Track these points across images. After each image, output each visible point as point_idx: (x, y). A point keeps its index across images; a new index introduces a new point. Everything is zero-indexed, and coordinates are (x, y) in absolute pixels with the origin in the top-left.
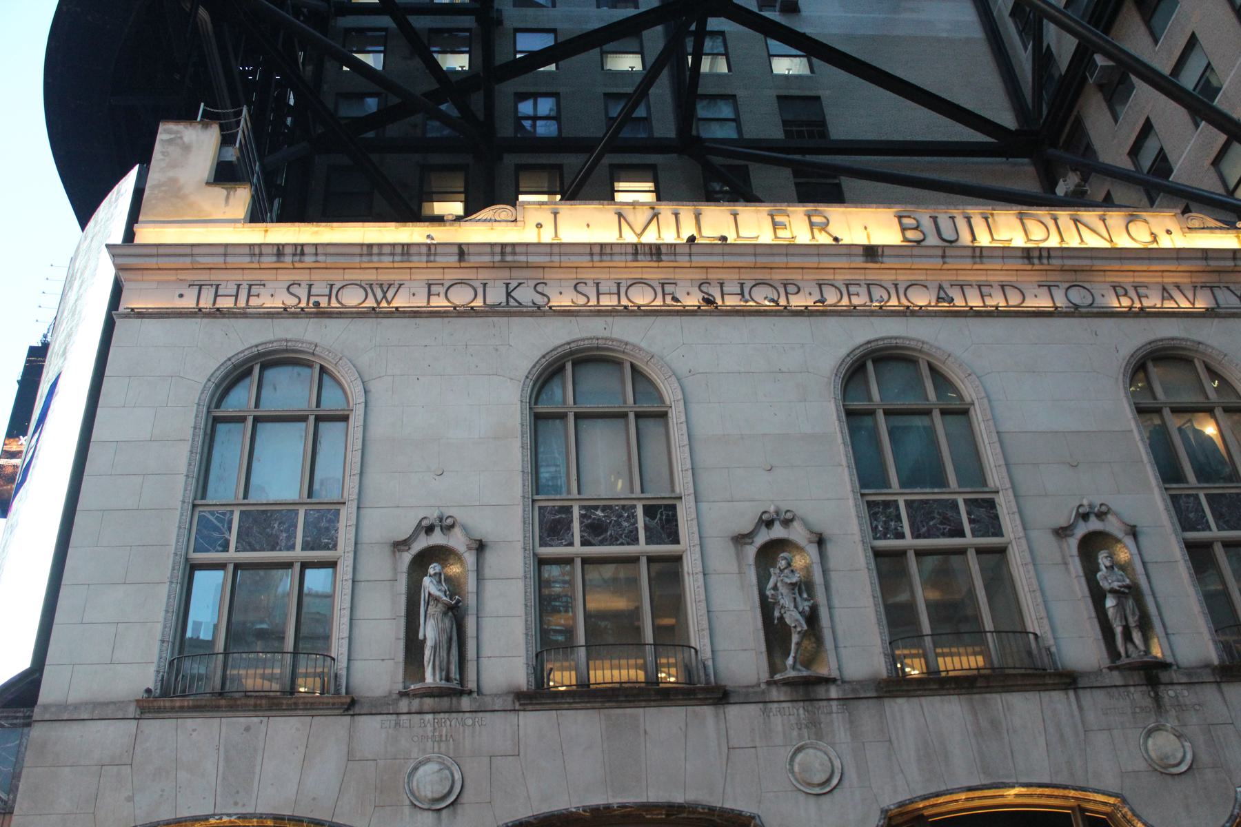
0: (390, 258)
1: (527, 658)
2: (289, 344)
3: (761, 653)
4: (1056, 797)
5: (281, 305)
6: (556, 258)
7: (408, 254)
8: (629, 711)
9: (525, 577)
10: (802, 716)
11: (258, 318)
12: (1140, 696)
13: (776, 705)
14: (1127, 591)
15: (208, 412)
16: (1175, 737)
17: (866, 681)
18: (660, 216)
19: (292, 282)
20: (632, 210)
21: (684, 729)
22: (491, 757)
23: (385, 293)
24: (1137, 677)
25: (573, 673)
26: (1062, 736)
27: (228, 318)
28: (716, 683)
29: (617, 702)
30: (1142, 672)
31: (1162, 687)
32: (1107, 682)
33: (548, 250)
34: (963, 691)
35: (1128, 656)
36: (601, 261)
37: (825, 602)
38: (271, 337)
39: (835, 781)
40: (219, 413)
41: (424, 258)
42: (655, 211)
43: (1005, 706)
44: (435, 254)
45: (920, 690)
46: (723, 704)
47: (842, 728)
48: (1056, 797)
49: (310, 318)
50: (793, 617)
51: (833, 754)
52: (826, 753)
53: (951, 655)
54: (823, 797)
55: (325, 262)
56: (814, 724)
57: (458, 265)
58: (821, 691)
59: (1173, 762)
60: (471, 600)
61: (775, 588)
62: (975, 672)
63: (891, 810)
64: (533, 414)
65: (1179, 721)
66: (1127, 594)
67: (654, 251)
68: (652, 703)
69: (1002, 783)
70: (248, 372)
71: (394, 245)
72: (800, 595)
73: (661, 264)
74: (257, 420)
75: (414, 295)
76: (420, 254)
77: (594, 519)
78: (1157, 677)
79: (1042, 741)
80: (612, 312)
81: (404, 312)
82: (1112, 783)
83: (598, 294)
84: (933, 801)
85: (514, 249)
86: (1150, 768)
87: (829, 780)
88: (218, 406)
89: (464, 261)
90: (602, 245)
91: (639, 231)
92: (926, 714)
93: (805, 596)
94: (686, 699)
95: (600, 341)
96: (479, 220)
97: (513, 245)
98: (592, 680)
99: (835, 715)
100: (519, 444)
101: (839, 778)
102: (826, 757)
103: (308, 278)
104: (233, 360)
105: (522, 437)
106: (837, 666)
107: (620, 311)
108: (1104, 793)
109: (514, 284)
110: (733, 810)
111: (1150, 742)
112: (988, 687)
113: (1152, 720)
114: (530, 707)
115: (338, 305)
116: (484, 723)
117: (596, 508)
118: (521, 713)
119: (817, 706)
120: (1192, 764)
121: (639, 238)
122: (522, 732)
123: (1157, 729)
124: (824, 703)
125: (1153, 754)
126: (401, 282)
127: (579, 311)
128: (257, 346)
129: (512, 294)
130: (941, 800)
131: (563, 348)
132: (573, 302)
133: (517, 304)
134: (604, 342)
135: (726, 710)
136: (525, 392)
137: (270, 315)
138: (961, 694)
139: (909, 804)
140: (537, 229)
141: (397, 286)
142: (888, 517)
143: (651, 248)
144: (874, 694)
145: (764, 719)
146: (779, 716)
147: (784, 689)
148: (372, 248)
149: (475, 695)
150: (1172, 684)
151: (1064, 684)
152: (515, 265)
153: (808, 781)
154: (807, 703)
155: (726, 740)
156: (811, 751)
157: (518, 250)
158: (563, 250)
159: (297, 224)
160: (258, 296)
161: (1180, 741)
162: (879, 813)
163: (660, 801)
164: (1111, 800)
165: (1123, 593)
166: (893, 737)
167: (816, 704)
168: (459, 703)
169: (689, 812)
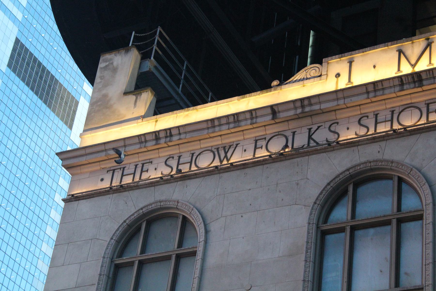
0: (226, 127)
2: (162, 204)
5: (325, 142)
6: (341, 102)
7: (238, 121)
11: (145, 187)
15: (318, 227)
18: (433, 45)
19: (169, 157)
20: (410, 45)
23: (226, 153)
27: (128, 191)
33: (334, 96)
36: (375, 97)
38: (152, 200)
40: (325, 227)
41: (249, 122)
42: (430, 41)
44: (256, 117)
49: (177, 181)
55: (185, 138)
57: (273, 122)
64: (319, 233)
67: (416, 79)
70: (345, 193)
71: (227, 116)
73: (425, 88)
74: (400, 221)
75: (245, 151)
76: (246, 119)
80: (386, 137)
81: (237, 166)
83: (376, 123)
85: (310, 101)
88: (326, 221)
89: (276, 118)
90: (374, 84)
91: (413, 62)
95: (372, 164)
96: (295, 81)
97: (309, 98)
100: (303, 258)
103: (178, 151)
104: (127, 222)
105: (307, 252)
107: (391, 135)
109: (315, 127)
115: (196, 168)
121: (413, 68)
126: (237, 143)
127: (359, 141)
128: (142, 209)
129: (313, 137)
131: (344, 175)
132: (356, 134)
133: (315, 144)
134: (375, 163)
136: (313, 215)
137: (154, 184)
140: (336, 79)
141: (235, 146)
143: (413, 78)
148: (214, 122)
152: (315, 113)
157: (313, 101)
158: (346, 94)
159: (175, 112)
160: (147, 171)
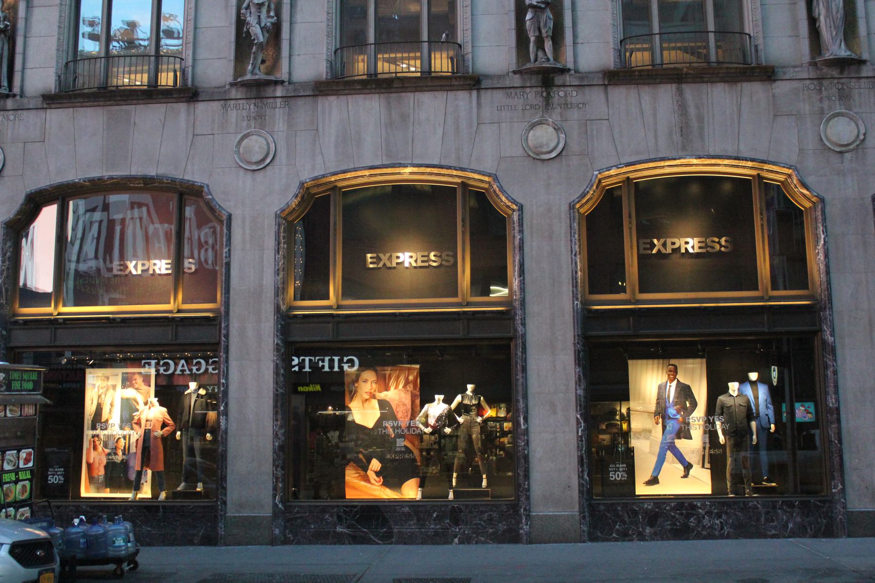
1: (57, 69)
3: (231, 60)
4: (444, 175)
8: (124, 107)
9: (61, 4)
10: (252, 110)
12: (533, 96)
13: (233, 102)
14: (543, 6)
16: (553, 130)
17: (310, 82)
21: (163, 121)
22: (25, 143)
24: (535, 80)
25: (418, 63)
26: (457, 128)
28: (472, 73)
29: (115, 101)
30: (540, 76)
31: (555, 89)
32: (508, 83)
34: (383, 90)
35: (536, 60)
37: (289, 19)
39: (268, 161)
43: (416, 103)
45: (347, 89)
46: (194, 101)
47: (281, 120)
48: (444, 175)
50: (256, 30)
51: (270, 139)
52: (266, 139)
53: (409, 59)
54: (258, 172)
56: (260, 117)
58: (269, 91)
59: (545, 150)
60: (21, 24)
61: (248, 8)
62: (394, 75)
63: (306, 182)
65: (561, 116)
66: (544, 9)
68: (141, 102)
69: (400, 164)
72: (268, 11)
78: (553, 79)
79: (440, 132)
82: (489, 165)
84: (341, 176)
86: (526, 155)
87: (263, 160)
93: (272, 14)
94: (166, 98)
98: (380, 70)
99: (277, 110)
101: (271, 157)
102: (265, 142)
106: (288, 71)
108: (479, 173)
110: (189, 181)
111: (532, 133)
112: (403, 87)
113: (538, 115)
114: (53, 106)
116: (22, 118)
118: (48, 111)
119: (265, 103)
120: (561, 152)
122: (47, 127)
123: (540, 123)
124: (271, 100)
125: (530, 143)
130: (349, 175)
135: (196, 106)
138: (382, 93)
139: (321, 178)
144: (310, 94)
145: (223, 112)
147: (241, 89)
149: (18, 97)
150: (564, 86)
151: (469, 85)
153: (249, 160)
154: (258, 101)
155: (192, 129)
156: (254, 137)
161: (557, 132)
162: (298, 184)
163: (139, 174)
164: (486, 179)
165: (540, 8)
167: (265, 101)
168: (5, 104)
169: (159, 183)
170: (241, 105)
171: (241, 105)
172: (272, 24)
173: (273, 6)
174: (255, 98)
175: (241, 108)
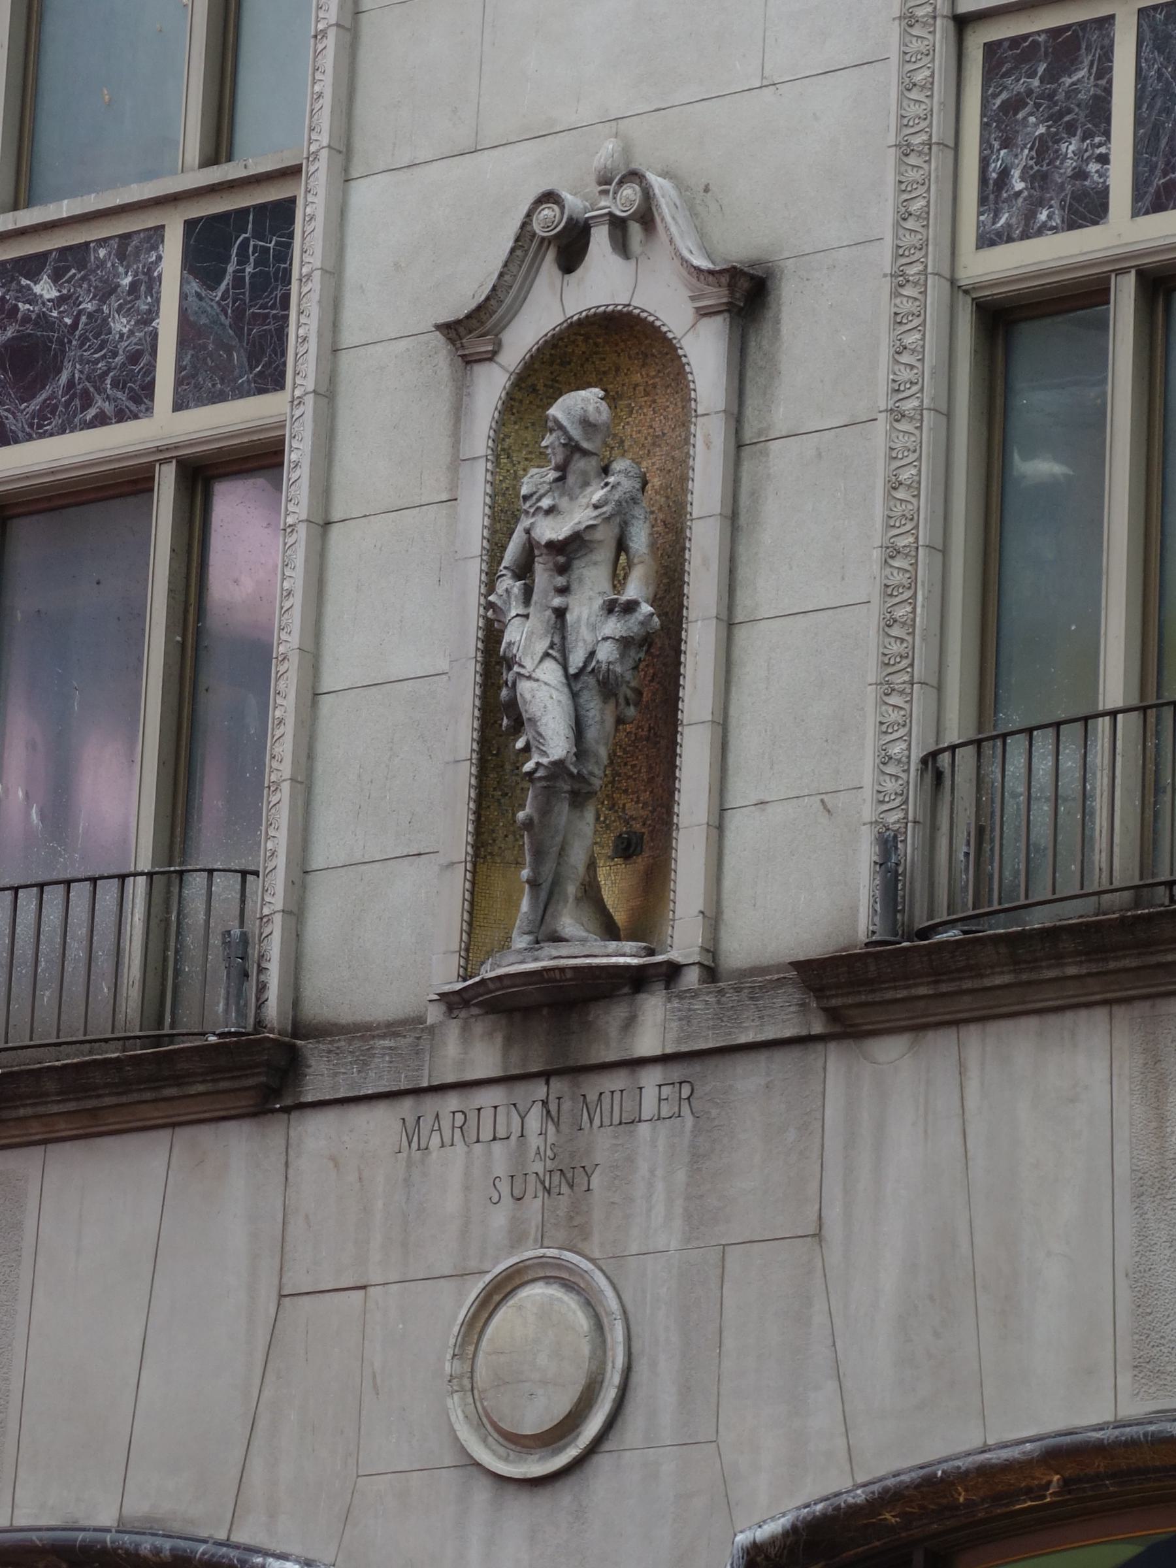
10: (534, 1141)
13: (453, 1101)
46: (287, 1110)
47: (660, 1186)
77: (26, 319)
92: (972, 1103)
99: (644, 1129)
102: (582, 1321)
117: (32, 266)
119: (592, 1097)
142: (1056, 118)
145: (409, 1163)
146: (460, 1147)
166: (834, 1214)
170: (487, 1114)
171: (487, 1114)
172: (625, 643)
173: (640, 539)
174: (546, 1076)
175: (486, 1135)
